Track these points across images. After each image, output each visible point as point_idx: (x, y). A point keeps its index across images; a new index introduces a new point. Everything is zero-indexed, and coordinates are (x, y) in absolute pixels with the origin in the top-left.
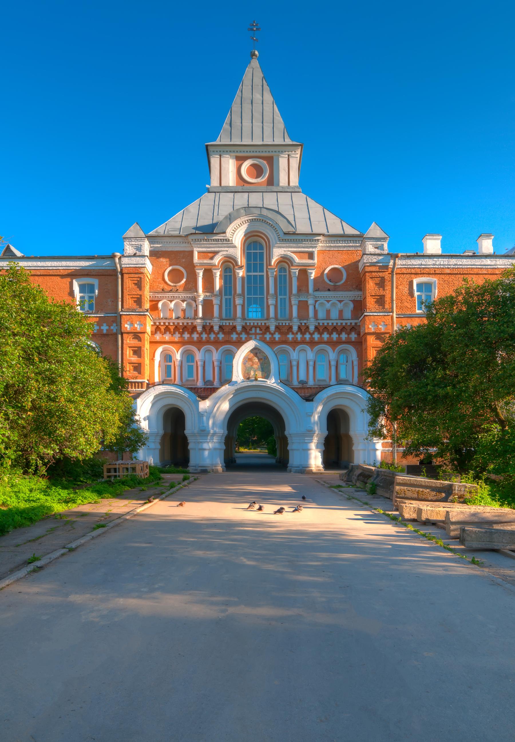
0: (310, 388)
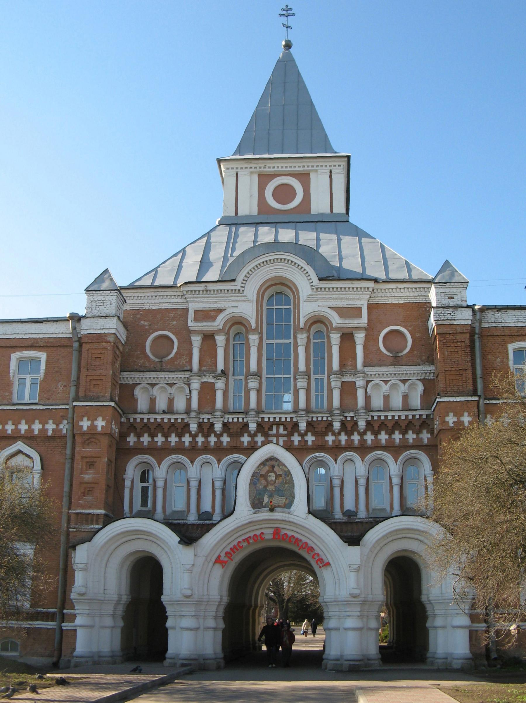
0: (361, 522)
